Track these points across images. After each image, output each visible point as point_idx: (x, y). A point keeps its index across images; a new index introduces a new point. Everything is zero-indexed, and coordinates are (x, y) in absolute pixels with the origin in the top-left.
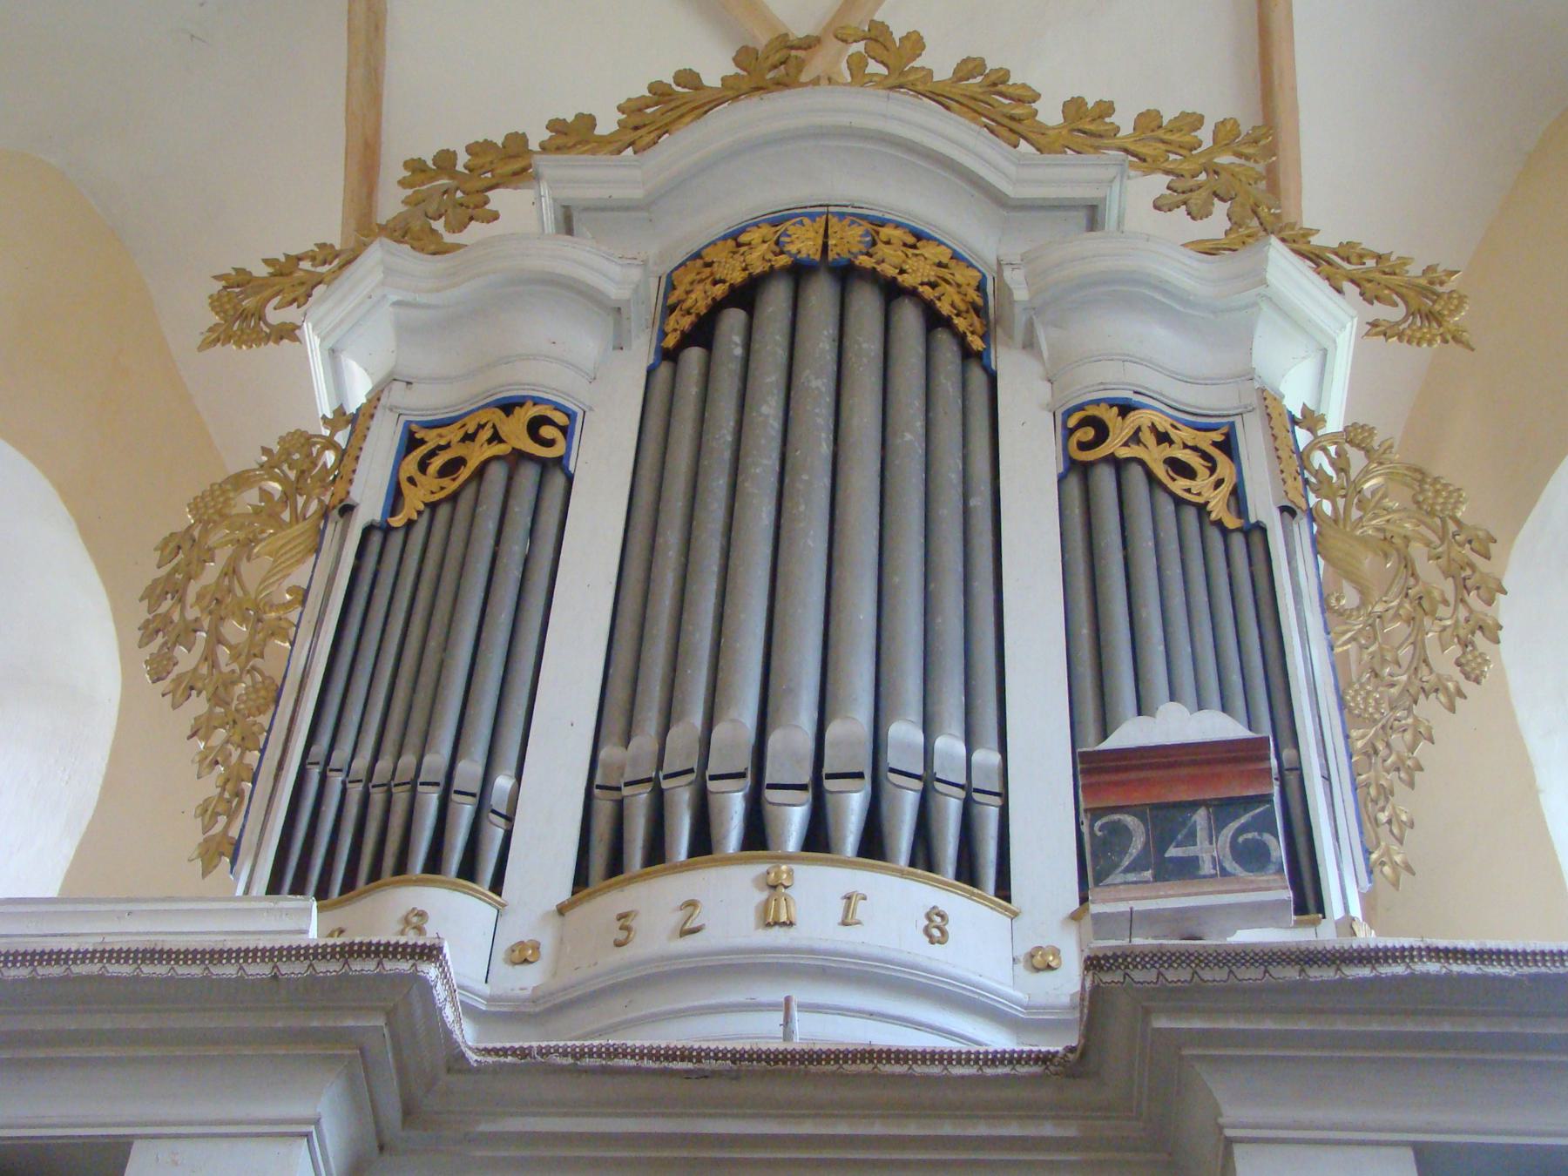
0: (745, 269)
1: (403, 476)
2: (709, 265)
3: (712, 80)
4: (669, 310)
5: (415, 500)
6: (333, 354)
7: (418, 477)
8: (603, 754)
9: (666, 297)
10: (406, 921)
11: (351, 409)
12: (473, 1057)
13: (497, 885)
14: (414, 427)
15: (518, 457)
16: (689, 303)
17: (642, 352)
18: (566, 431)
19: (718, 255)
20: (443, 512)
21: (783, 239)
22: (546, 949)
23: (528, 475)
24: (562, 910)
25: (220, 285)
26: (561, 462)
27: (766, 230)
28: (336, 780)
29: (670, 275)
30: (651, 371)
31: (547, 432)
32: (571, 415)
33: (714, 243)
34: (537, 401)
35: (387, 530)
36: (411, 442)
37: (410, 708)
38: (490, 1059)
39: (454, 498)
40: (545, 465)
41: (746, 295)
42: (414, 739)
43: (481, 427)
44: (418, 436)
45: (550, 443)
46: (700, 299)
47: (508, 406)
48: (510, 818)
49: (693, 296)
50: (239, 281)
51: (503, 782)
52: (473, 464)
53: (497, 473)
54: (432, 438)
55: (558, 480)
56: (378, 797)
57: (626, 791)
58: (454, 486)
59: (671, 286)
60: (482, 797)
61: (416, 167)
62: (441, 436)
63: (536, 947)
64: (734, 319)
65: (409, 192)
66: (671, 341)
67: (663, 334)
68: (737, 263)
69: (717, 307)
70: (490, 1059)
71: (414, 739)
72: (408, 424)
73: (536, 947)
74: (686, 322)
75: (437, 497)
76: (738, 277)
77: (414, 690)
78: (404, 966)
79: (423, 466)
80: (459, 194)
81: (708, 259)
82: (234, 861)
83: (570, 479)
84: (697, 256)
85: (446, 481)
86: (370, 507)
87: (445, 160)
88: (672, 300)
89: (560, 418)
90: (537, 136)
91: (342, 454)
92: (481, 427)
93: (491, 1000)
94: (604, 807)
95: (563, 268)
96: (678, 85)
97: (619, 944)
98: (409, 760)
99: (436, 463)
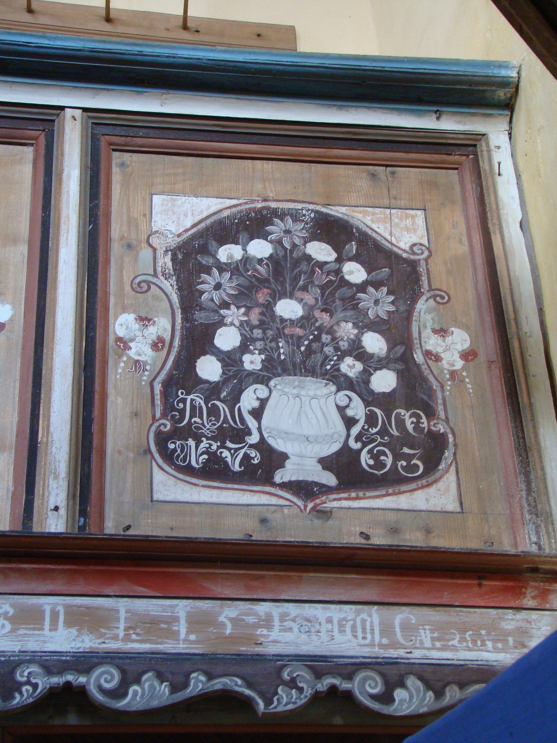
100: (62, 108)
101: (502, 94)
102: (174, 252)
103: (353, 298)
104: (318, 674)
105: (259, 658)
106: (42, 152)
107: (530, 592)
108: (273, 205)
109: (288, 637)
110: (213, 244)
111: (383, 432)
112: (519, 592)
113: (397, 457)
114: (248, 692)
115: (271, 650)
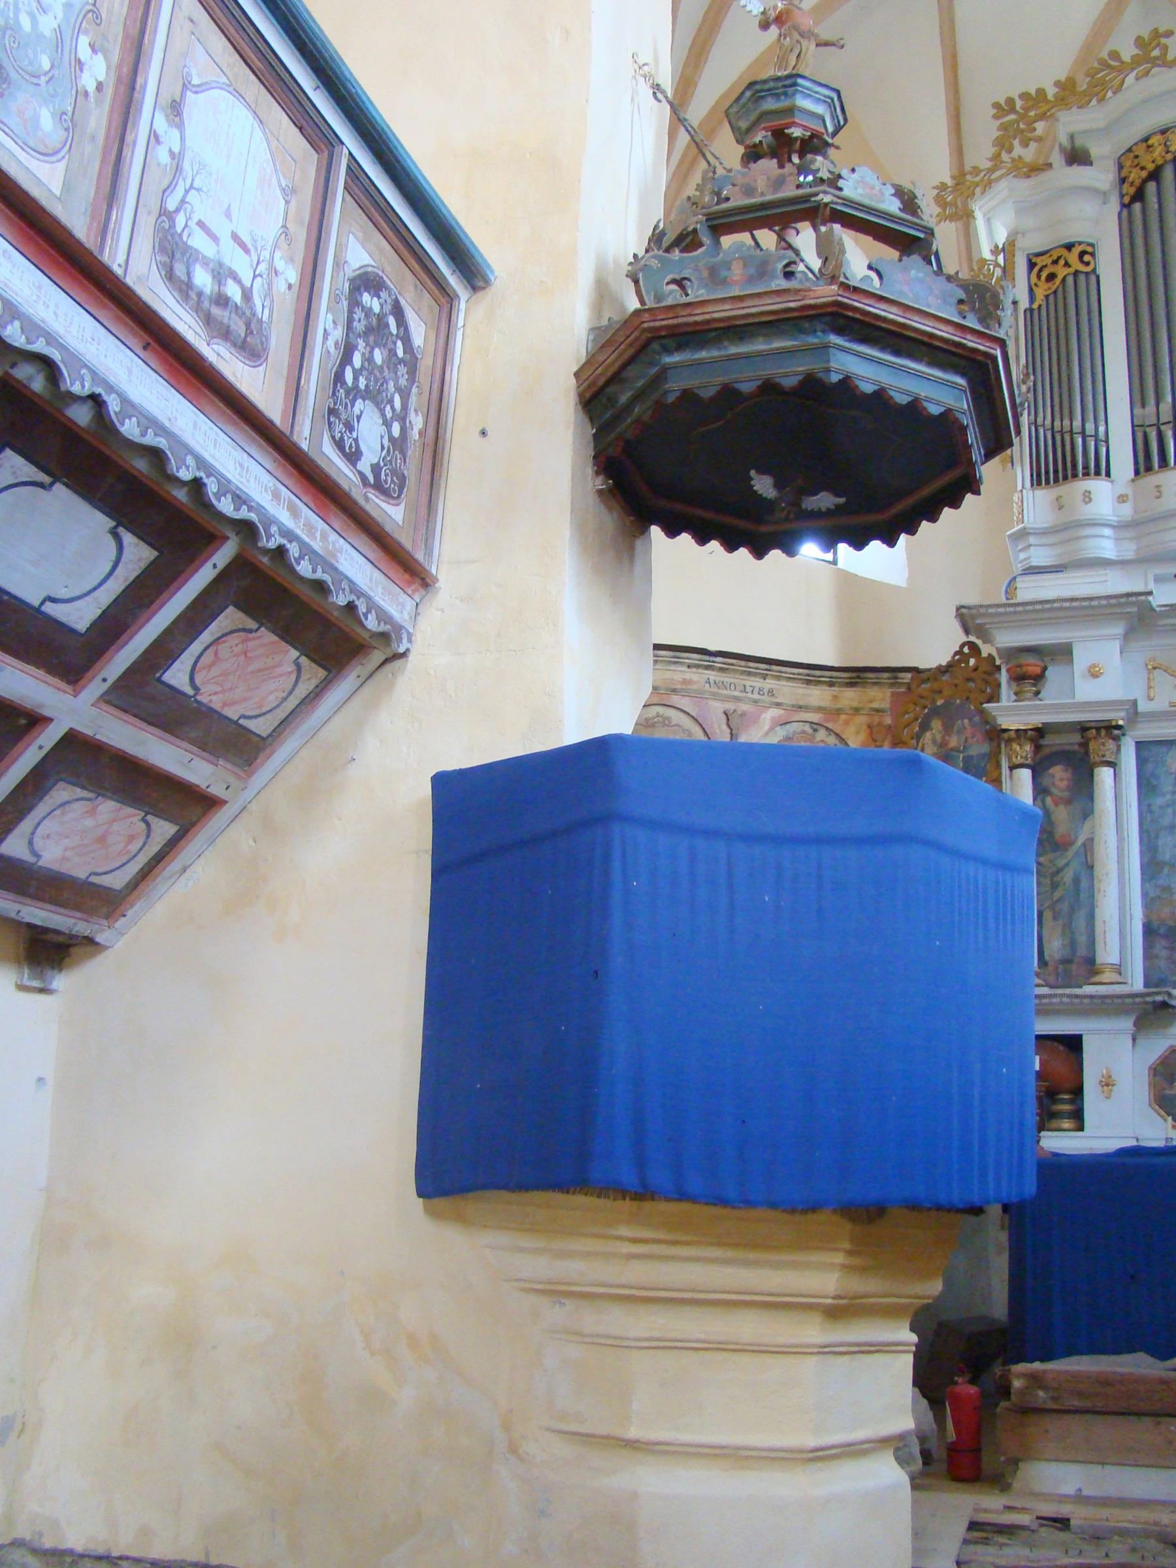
0: (1153, 162)
1: (1033, 283)
2: (1137, 157)
3: (1126, 57)
4: (1123, 181)
5: (1040, 294)
6: (988, 221)
7: (1039, 283)
8: (1135, 412)
9: (1119, 173)
10: (1084, 495)
11: (1001, 246)
12: (1158, 609)
13: (1108, 474)
14: (1031, 257)
15: (1076, 273)
16: (1131, 179)
17: (1114, 206)
18: (1093, 255)
19: (1140, 150)
20: (1051, 298)
21: (1168, 143)
22: (1131, 497)
23: (1082, 278)
24: (1133, 481)
25: (936, 192)
26: (1094, 270)
27: (1159, 137)
28: (1041, 431)
29: (1119, 158)
30: (1120, 214)
31: (1087, 258)
32: (1092, 245)
33: (1136, 144)
34: (1080, 243)
35: (1031, 310)
36: (1031, 265)
37: (1061, 396)
38: (1163, 609)
39: (1055, 292)
40: (1087, 274)
41: (1155, 175)
42: (1066, 412)
43: (1059, 258)
44: (1033, 261)
45: (1087, 264)
46: (1136, 176)
47: (1069, 247)
48: (1107, 442)
49: (1132, 175)
50: (942, 187)
51: (1102, 429)
52: (1060, 278)
53: (1070, 280)
54: (1040, 261)
55: (1093, 278)
56: (1058, 437)
57: (1148, 430)
58: (1055, 287)
59: (1121, 167)
60: (1096, 436)
61: (996, 105)
62: (1043, 261)
63: (1127, 496)
64: (1151, 187)
65: (998, 123)
66: (1127, 200)
67: (1122, 196)
68: (1149, 157)
69: (1145, 181)
70: (1163, 609)
71: (1066, 412)
72: (1028, 255)
73: (1127, 496)
74: (1132, 191)
75: (1048, 293)
76: (1151, 167)
77: (1060, 387)
78: (1143, 598)
79: (1039, 277)
80: (1022, 126)
81: (1137, 153)
82: (1013, 465)
83: (1098, 278)
84: (1130, 150)
85: (1050, 284)
86: (1024, 304)
87: (1010, 101)
88: (1123, 174)
89: (1089, 249)
90: (1051, 92)
91: (1004, 270)
92: (1059, 258)
93: (1118, 522)
94: (1140, 436)
95: (1085, 182)
96: (1111, 59)
97: (1158, 497)
98: (1066, 422)
99: (1044, 275)
100: (343, 143)
101: (481, 284)
102: (352, 281)
103: (395, 366)
104: (351, 592)
105: (336, 569)
106: (325, 163)
107: (413, 587)
108: (385, 278)
109: (345, 563)
110: (362, 289)
111: (390, 461)
112: (410, 583)
113: (392, 481)
114: (332, 587)
115: (340, 568)
